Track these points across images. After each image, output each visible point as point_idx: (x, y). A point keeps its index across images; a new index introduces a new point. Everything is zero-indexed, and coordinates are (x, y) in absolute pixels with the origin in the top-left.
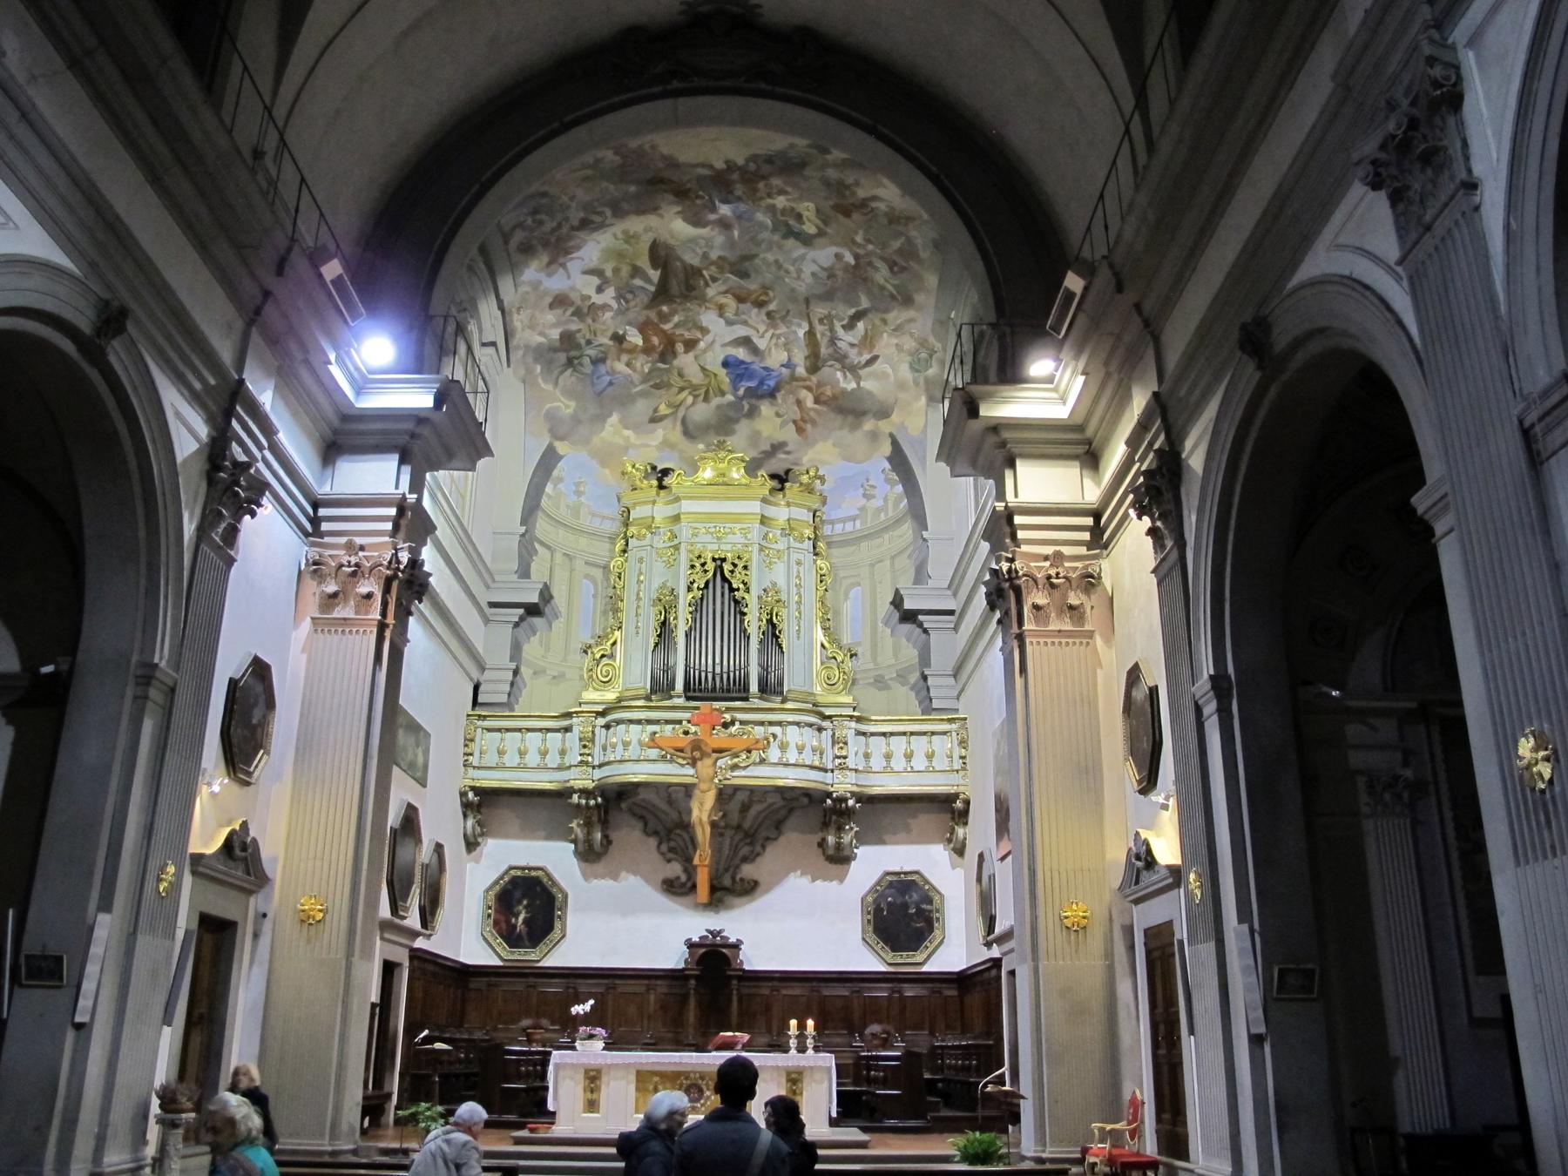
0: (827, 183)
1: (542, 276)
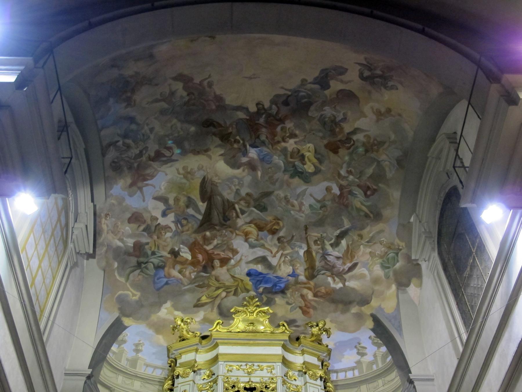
1: (125, 194)
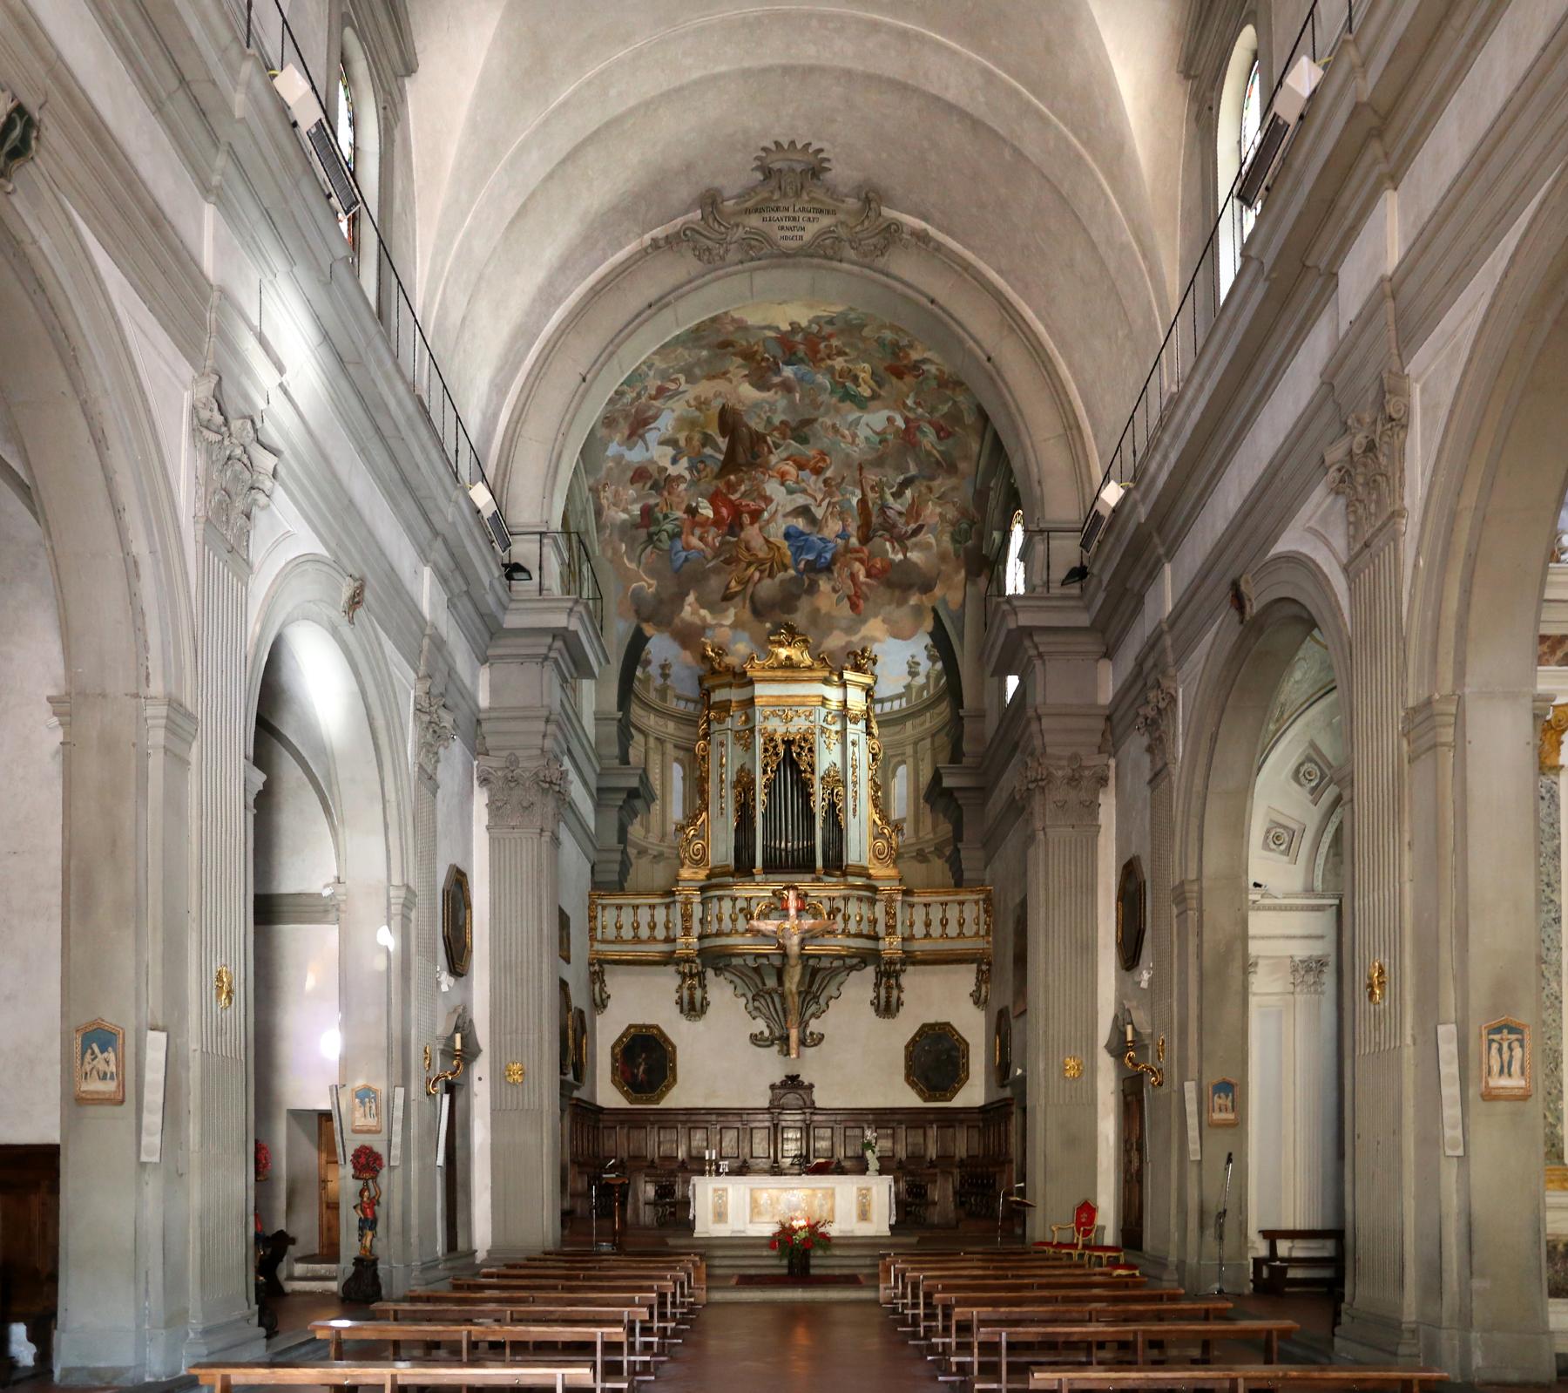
0: (881, 342)
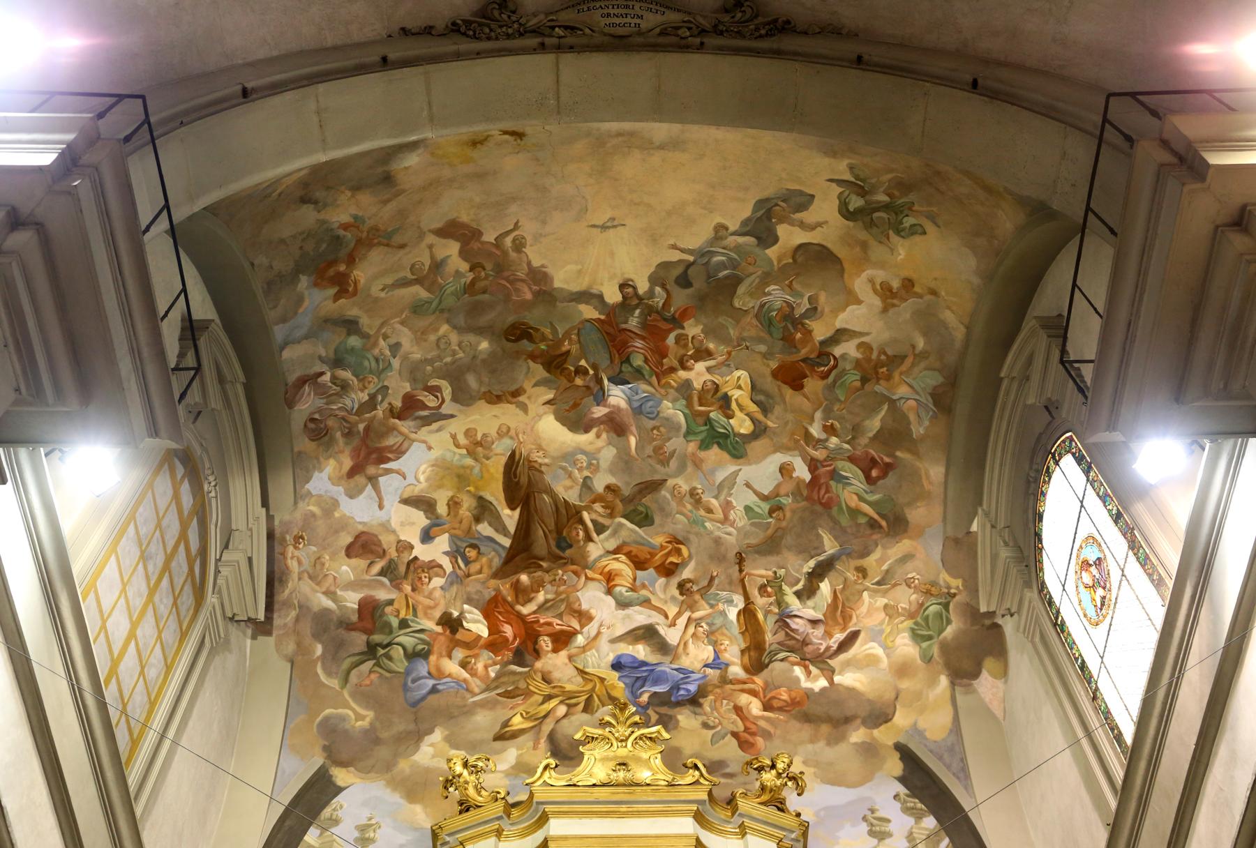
1: (338, 491)
